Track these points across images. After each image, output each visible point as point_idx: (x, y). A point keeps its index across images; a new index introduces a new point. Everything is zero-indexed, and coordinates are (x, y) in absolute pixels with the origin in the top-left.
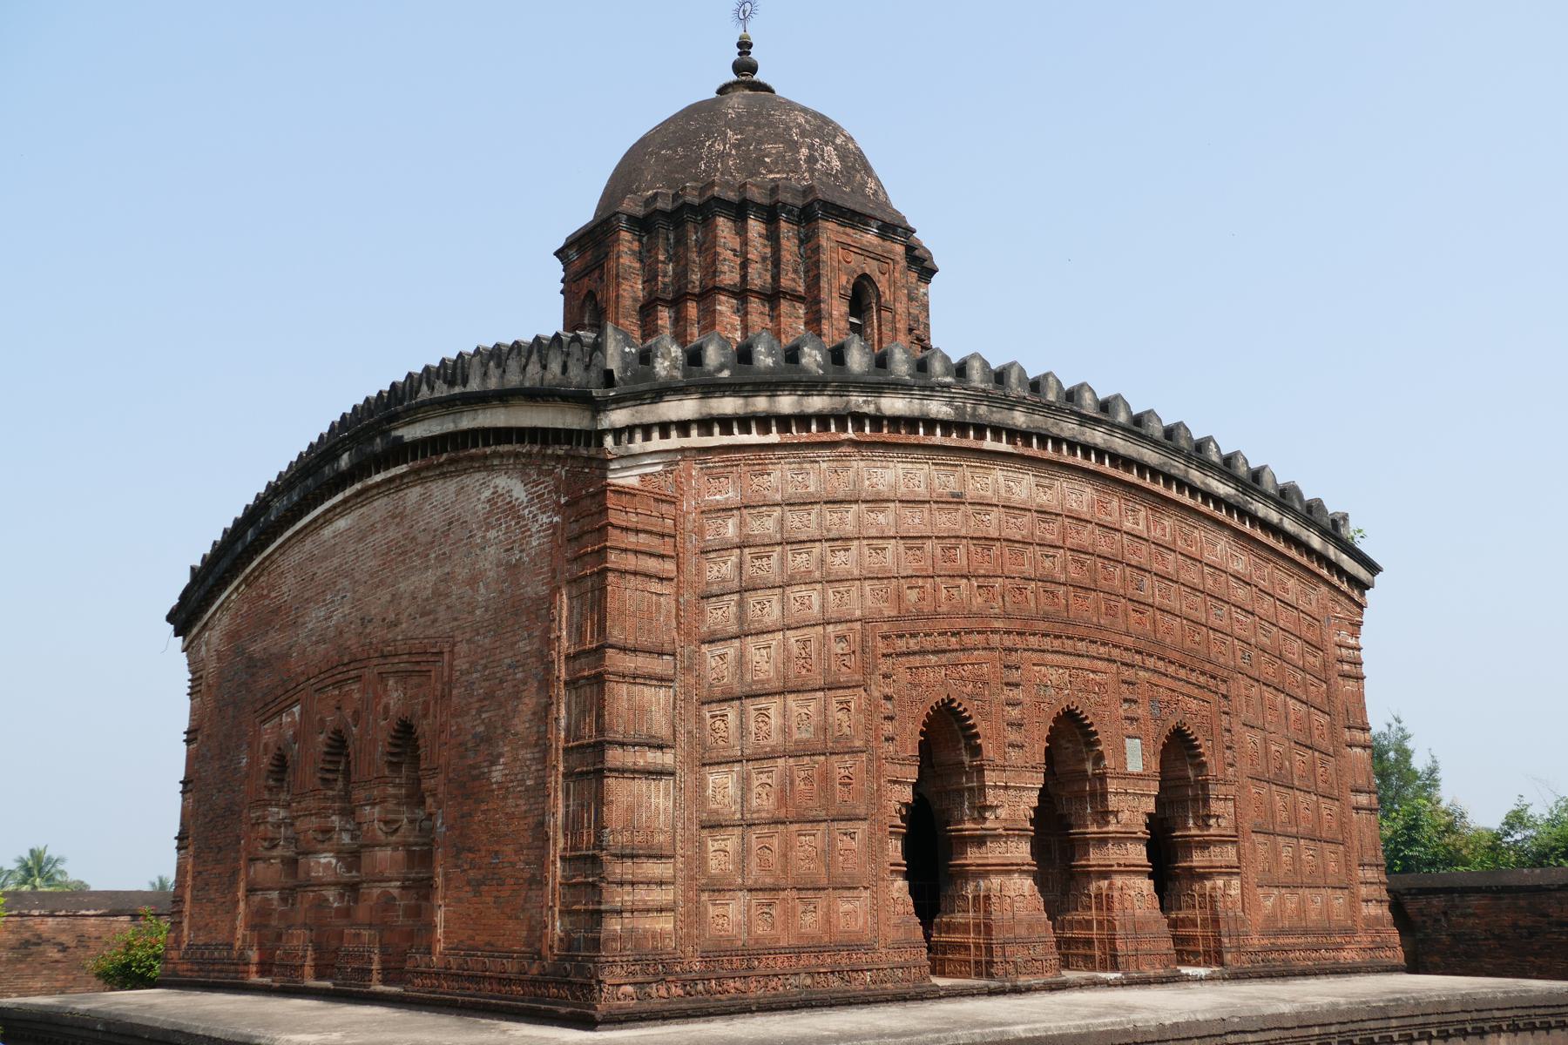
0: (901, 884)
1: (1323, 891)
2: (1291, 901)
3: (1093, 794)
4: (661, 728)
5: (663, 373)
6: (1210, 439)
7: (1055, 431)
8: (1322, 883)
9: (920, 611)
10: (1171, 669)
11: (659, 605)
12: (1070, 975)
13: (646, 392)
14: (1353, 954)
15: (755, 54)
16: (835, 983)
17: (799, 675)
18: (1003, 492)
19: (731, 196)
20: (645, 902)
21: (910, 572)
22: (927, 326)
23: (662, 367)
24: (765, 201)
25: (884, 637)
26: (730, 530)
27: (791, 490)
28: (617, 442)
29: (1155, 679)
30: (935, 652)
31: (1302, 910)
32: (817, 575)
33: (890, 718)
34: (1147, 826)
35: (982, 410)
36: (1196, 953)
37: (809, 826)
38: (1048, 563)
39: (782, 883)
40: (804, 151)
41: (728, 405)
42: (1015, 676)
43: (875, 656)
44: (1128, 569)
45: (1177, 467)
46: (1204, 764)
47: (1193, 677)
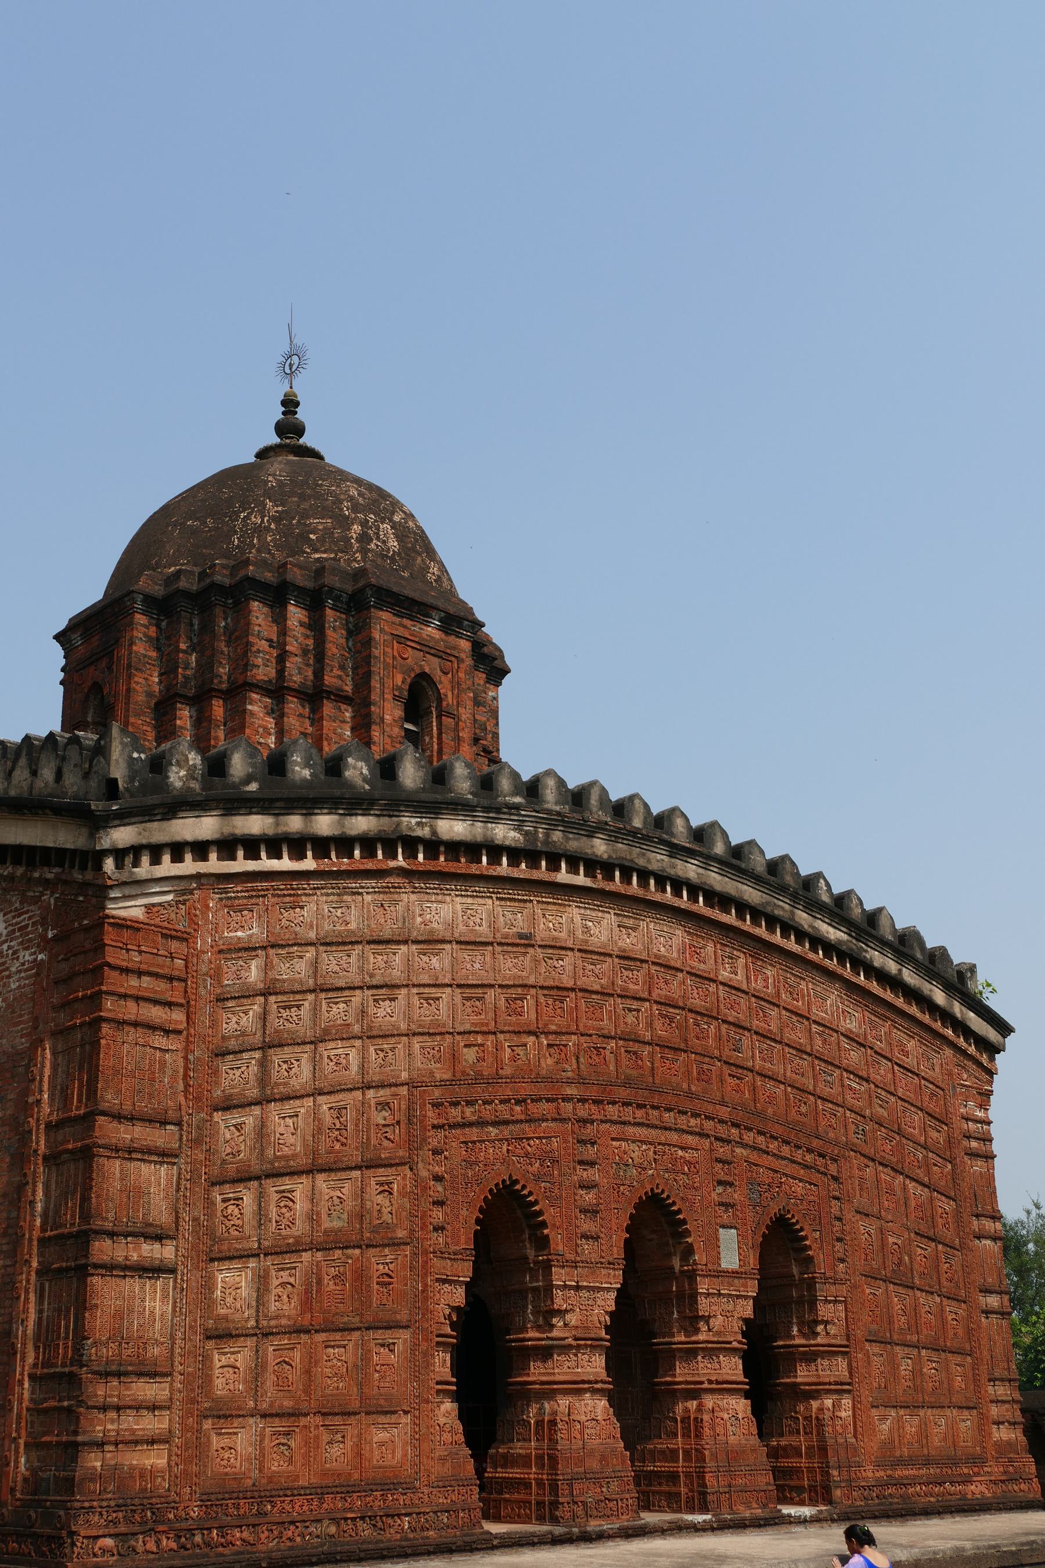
0: (449, 1406)
1: (948, 1412)
2: (911, 1426)
3: (680, 1295)
4: (160, 1213)
5: (178, 784)
6: (819, 875)
7: (641, 862)
8: (946, 1403)
9: (479, 1074)
10: (773, 1146)
11: (163, 1063)
12: (650, 1518)
13: (155, 806)
14: (982, 1488)
15: (301, 414)
16: (365, 1531)
17: (331, 1151)
18: (579, 933)
19: (269, 576)
20: (133, 1431)
21: (468, 1027)
22: (496, 736)
23: (176, 777)
24: (309, 584)
25: (436, 1105)
26: (253, 973)
27: (327, 927)
28: (120, 865)
29: (754, 1157)
30: (495, 1124)
31: (923, 1434)
32: (356, 1029)
33: (440, 1203)
34: (744, 1334)
35: (557, 836)
36: (800, 1489)
37: (338, 1336)
38: (630, 1018)
39: (304, 1407)
41: (255, 824)
42: (591, 1152)
43: (424, 1129)
44: (724, 1027)
45: (782, 907)
46: (810, 1259)
47: (799, 1156)
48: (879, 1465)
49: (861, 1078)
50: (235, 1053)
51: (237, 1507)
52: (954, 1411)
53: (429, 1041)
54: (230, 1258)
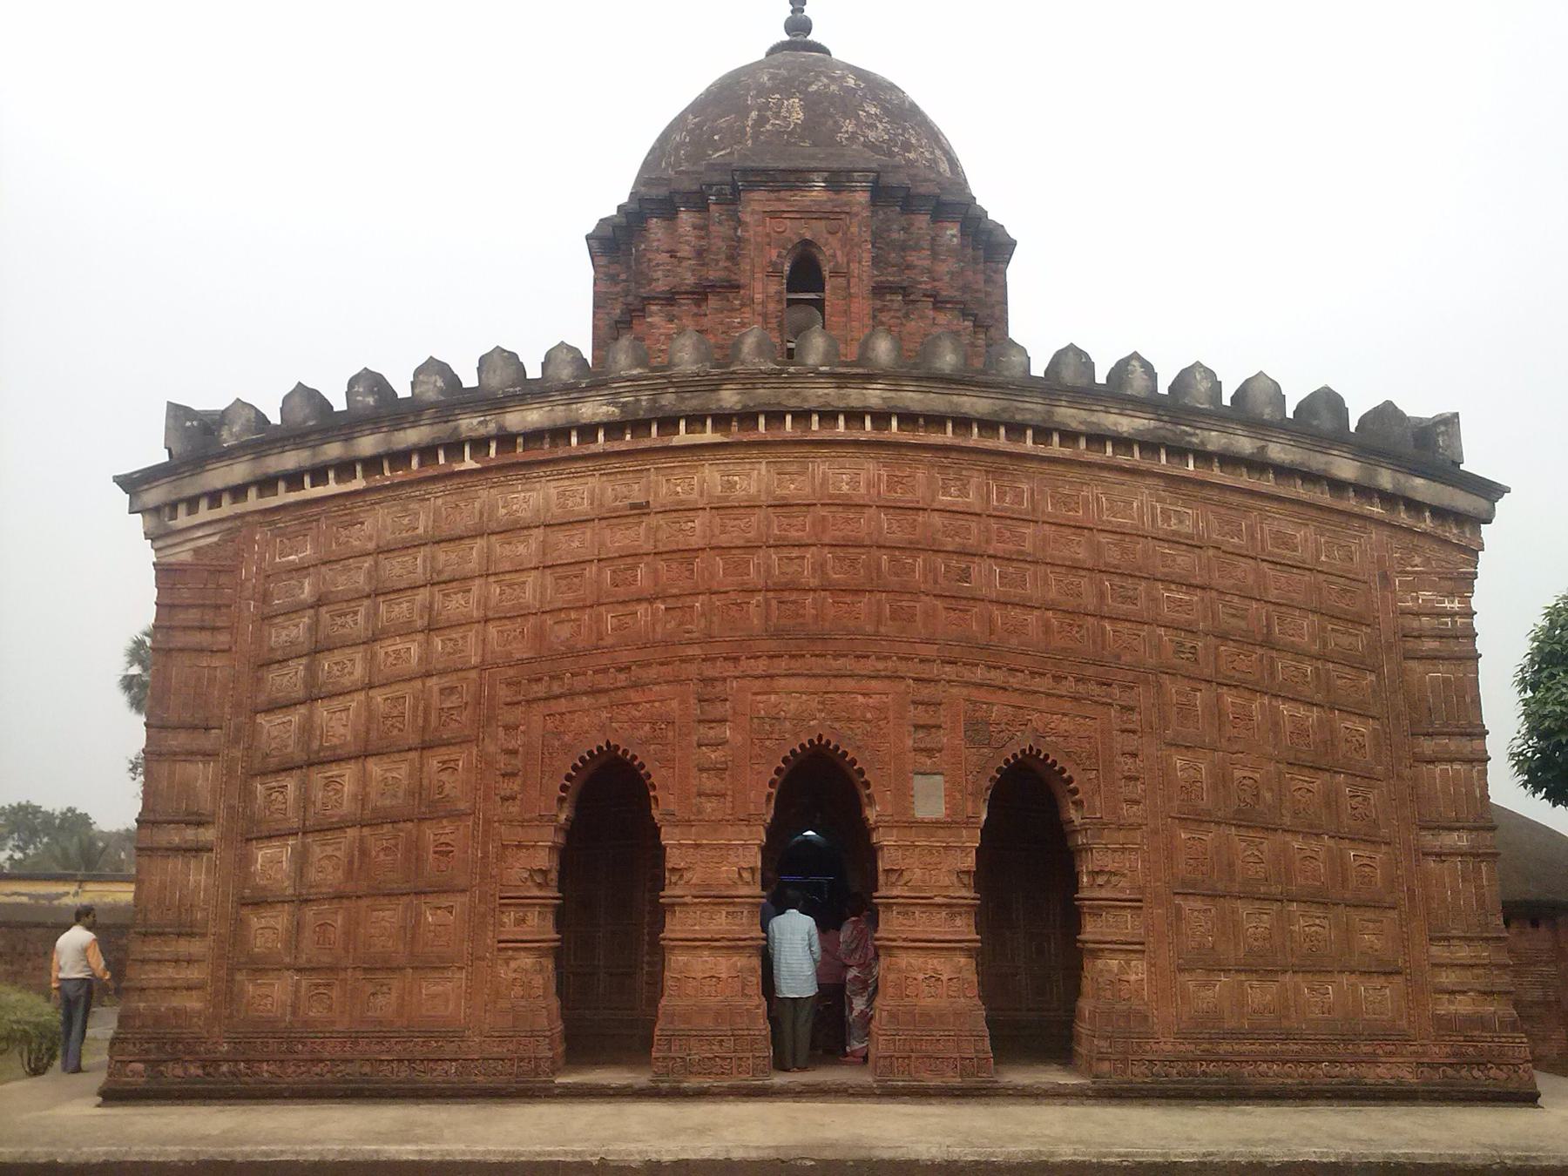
2: (1260, 994)
4: (206, 803)
7: (793, 403)
12: (779, 1079)
16: (404, 1072)
21: (559, 605)
26: (307, 591)
27: (389, 536)
29: (976, 694)
30: (586, 693)
35: (668, 399)
37: (385, 901)
38: (792, 568)
40: (754, 114)
44: (939, 560)
48: (1183, 1036)
49: (1189, 586)
50: (279, 662)
51: (266, 1044)
53: (508, 625)
54: (270, 837)
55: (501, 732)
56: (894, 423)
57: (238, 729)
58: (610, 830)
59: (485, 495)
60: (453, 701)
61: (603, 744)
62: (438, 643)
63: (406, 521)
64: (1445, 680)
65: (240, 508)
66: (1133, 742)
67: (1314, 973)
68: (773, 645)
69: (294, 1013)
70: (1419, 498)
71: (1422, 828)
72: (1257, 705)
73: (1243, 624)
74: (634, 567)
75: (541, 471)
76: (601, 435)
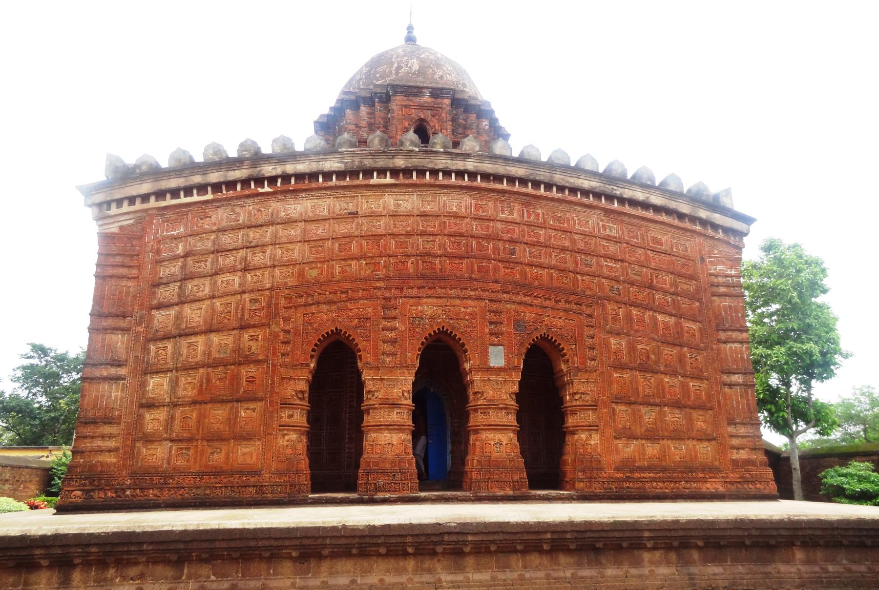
2: (652, 449)
7: (430, 166)
12: (423, 494)
20: (99, 446)
29: (518, 307)
30: (325, 303)
42: (393, 313)
43: (277, 309)
44: (500, 244)
48: (617, 469)
50: (164, 284)
51: (152, 480)
52: (694, 442)
53: (285, 269)
54: (157, 373)
55: (281, 322)
56: (479, 178)
57: (141, 317)
58: (336, 373)
59: (274, 205)
60: (257, 306)
61: (334, 329)
62: (249, 276)
63: (233, 217)
64: (730, 307)
65: (146, 206)
66: (592, 331)
67: (676, 439)
68: (420, 282)
69: (169, 462)
70: (717, 222)
71: (723, 373)
72: (648, 314)
73: (639, 278)
74: (351, 242)
75: (303, 194)
76: (334, 177)
